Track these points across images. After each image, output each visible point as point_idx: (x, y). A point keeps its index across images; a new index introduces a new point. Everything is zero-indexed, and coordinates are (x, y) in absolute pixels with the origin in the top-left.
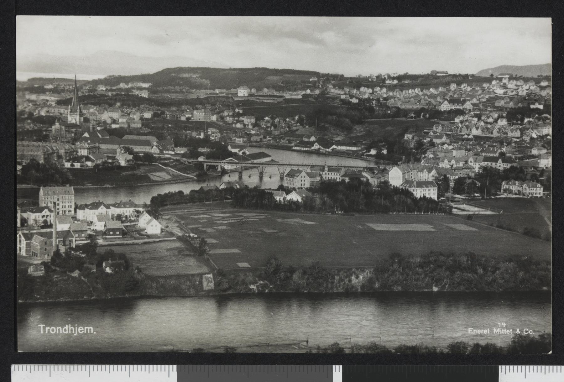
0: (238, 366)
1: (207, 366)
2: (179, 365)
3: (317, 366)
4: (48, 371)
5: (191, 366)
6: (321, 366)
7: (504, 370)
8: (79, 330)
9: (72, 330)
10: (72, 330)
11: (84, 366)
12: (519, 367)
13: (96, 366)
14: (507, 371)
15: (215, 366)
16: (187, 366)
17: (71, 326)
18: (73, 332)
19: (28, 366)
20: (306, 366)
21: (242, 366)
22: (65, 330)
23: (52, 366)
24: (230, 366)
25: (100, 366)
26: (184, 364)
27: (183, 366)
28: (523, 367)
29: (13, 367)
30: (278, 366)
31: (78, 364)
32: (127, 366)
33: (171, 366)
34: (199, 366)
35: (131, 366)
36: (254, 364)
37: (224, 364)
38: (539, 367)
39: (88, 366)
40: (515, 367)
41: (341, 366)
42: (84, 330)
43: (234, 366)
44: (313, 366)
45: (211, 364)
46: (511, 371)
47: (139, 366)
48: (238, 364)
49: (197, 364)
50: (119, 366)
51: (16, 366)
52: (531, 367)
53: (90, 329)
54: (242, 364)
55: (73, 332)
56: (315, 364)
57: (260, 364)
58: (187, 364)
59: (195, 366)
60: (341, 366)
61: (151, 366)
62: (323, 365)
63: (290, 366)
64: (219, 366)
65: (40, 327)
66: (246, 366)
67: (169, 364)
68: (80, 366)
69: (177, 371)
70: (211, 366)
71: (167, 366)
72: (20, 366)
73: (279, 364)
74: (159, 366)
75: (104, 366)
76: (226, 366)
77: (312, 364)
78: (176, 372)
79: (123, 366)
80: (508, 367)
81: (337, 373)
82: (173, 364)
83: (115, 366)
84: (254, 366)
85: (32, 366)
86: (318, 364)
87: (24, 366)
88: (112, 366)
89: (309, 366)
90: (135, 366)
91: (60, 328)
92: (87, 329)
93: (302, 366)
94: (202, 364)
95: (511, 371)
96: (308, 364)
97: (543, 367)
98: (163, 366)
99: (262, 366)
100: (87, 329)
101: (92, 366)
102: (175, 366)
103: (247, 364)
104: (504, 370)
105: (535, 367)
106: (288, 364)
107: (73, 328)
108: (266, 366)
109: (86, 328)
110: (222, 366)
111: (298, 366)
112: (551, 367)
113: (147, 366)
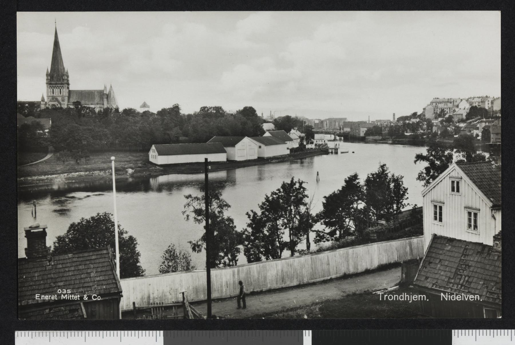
3: (289, 331)
4: (48, 337)
5: (176, 331)
6: (293, 331)
7: (456, 334)
8: (414, 297)
9: (407, 297)
10: (407, 297)
11: (80, 332)
12: (471, 331)
13: (91, 332)
14: (460, 334)
15: (197, 332)
16: (172, 331)
17: (406, 295)
18: (409, 299)
19: (30, 332)
20: (279, 331)
21: (222, 331)
22: (402, 298)
23: (51, 332)
24: (211, 332)
25: (94, 332)
26: (170, 329)
27: (169, 331)
29: (16, 333)
32: (119, 332)
33: (158, 332)
34: (183, 331)
35: (122, 332)
36: (233, 329)
37: (205, 330)
38: (488, 331)
39: (84, 332)
41: (311, 331)
42: (418, 298)
43: (215, 332)
45: (194, 330)
46: (463, 334)
47: (130, 332)
48: (218, 329)
49: (181, 330)
50: (112, 332)
51: (20, 332)
52: (481, 331)
53: (424, 297)
54: (222, 329)
55: (409, 299)
56: (287, 329)
57: (238, 329)
60: (311, 331)
61: (140, 332)
62: (295, 330)
63: (265, 331)
64: (201, 331)
66: (225, 331)
68: (76, 332)
69: (164, 336)
70: (194, 331)
71: (154, 332)
72: (23, 332)
73: (255, 330)
74: (147, 332)
75: (98, 332)
76: (208, 332)
78: (163, 337)
79: (115, 332)
80: (460, 331)
81: (307, 337)
82: (159, 329)
83: (108, 332)
84: (233, 331)
85: (34, 332)
87: (27, 332)
88: (105, 332)
90: (126, 332)
92: (421, 297)
93: (275, 331)
94: (186, 330)
95: (463, 334)
96: (282, 329)
97: (492, 331)
98: (151, 332)
99: (240, 331)
100: (421, 297)
101: (87, 332)
102: (162, 332)
103: (227, 329)
104: (456, 334)
106: (263, 330)
110: (204, 331)
111: (272, 331)
112: (499, 331)
113: (137, 332)
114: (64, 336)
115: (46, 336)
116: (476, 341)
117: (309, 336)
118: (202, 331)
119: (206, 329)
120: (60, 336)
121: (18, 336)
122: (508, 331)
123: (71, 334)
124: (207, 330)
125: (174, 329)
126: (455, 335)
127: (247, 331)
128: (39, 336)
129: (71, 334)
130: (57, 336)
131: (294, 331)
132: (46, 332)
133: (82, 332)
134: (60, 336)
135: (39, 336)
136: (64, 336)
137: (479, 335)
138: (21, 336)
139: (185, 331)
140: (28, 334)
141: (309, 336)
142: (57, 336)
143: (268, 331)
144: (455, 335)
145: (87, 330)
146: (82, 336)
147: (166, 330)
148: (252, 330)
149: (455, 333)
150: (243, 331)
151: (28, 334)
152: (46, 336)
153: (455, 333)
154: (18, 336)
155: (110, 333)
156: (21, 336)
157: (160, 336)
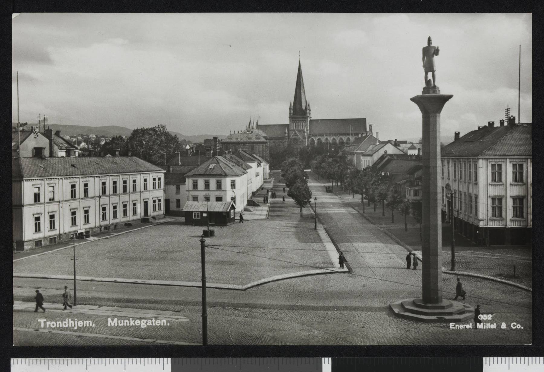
0: (231, 358)
1: (200, 359)
3: (307, 359)
4: (47, 364)
5: (185, 359)
6: (311, 359)
7: (488, 362)
11: (81, 359)
13: (92, 359)
14: (492, 362)
15: (208, 359)
16: (181, 359)
20: (296, 359)
21: (235, 359)
23: (46, 359)
24: (223, 359)
25: (96, 359)
26: (177, 357)
27: (177, 359)
28: (507, 358)
29: (13, 360)
30: (269, 359)
32: (123, 359)
33: (165, 359)
34: (192, 359)
35: (127, 359)
38: (522, 358)
39: (85, 359)
40: (499, 358)
43: (227, 359)
45: (204, 357)
47: (135, 359)
49: (190, 357)
50: (115, 359)
51: (15, 359)
52: (515, 358)
56: (305, 356)
57: (251, 357)
58: (181, 357)
59: (188, 359)
61: (146, 359)
64: (211, 359)
65: (40, 323)
66: (238, 359)
67: (163, 357)
68: (77, 359)
69: (171, 364)
70: (204, 359)
71: (162, 359)
72: (19, 359)
73: (270, 357)
74: (154, 359)
75: (100, 359)
76: (219, 359)
77: (302, 357)
78: (171, 365)
79: (119, 359)
81: (327, 365)
82: (167, 357)
85: (31, 359)
86: (308, 357)
87: (23, 359)
88: (108, 359)
90: (131, 359)
91: (60, 322)
93: (292, 359)
97: (526, 358)
98: (158, 359)
99: (254, 359)
102: (169, 359)
103: (240, 356)
104: (488, 362)
105: (519, 358)
106: (279, 357)
107: (73, 322)
109: (85, 322)
110: (215, 359)
112: (534, 358)
113: (142, 359)
114: (64, 364)
115: (44, 364)
116: (509, 369)
117: (329, 364)
119: (218, 356)
120: (60, 364)
123: (71, 362)
126: (486, 363)
127: (261, 359)
128: (37, 364)
129: (71, 362)
130: (56, 364)
132: (44, 360)
133: (83, 359)
135: (37, 364)
136: (64, 364)
137: (513, 363)
138: (18, 364)
139: (195, 358)
141: (329, 364)
142: (56, 364)
144: (486, 363)
145: (88, 357)
146: (83, 364)
147: (174, 357)
148: (267, 357)
149: (486, 360)
150: (257, 359)
152: (44, 364)
153: (486, 360)
155: (113, 360)
156: (18, 364)
157: (167, 364)
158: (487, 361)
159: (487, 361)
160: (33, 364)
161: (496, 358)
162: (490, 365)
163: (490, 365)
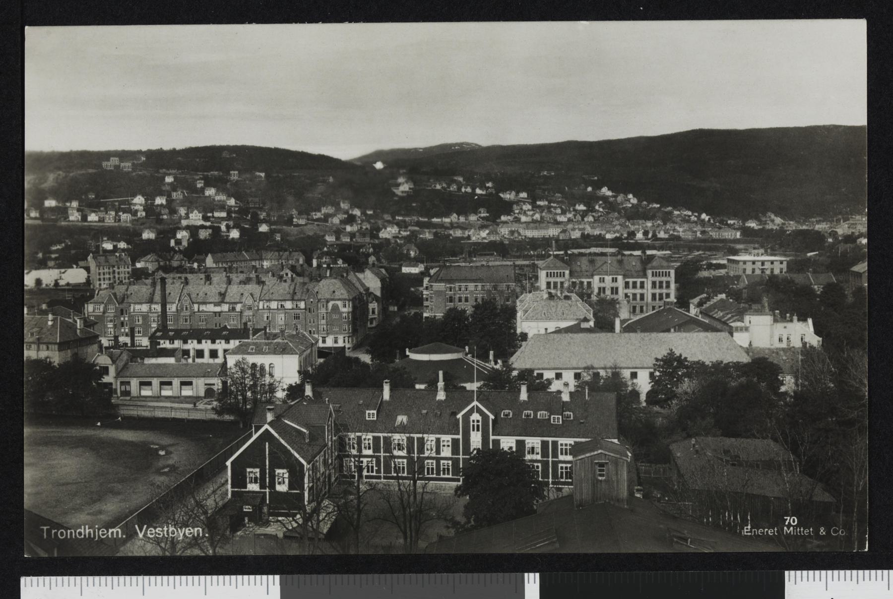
0: (376, 575)
1: (327, 577)
2: (284, 576)
3: (501, 575)
4: (78, 586)
5: (302, 577)
7: (792, 578)
12: (817, 572)
14: (799, 579)
15: (339, 576)
16: (296, 576)
19: (47, 578)
20: (482, 575)
21: (383, 576)
24: (364, 576)
27: (290, 577)
29: (23, 580)
31: (125, 575)
32: (202, 577)
33: (271, 577)
34: (314, 576)
35: (209, 577)
38: (848, 572)
39: (140, 578)
40: (811, 572)
41: (537, 575)
43: (370, 576)
44: (494, 575)
46: (805, 579)
48: (376, 572)
49: (311, 573)
51: (28, 579)
54: (382, 573)
58: (297, 574)
59: (308, 577)
60: (537, 575)
63: (457, 575)
64: (345, 576)
66: (389, 576)
67: (267, 574)
68: (128, 578)
69: (280, 585)
70: (333, 576)
72: (35, 579)
73: (439, 573)
76: (358, 576)
78: (279, 587)
81: (532, 584)
82: (274, 573)
84: (401, 576)
88: (178, 577)
89: (488, 575)
90: (215, 577)
93: (476, 575)
94: (319, 573)
95: (805, 579)
98: (258, 577)
99: (413, 576)
101: (147, 578)
102: (277, 577)
103: (391, 572)
104: (792, 578)
106: (453, 573)
108: (419, 576)
112: (867, 572)
117: (535, 583)
118: (347, 575)
120: (100, 586)
121: (25, 586)
122: (882, 572)
124: (357, 573)
125: (299, 573)
126: (789, 581)
127: (426, 575)
128: (63, 586)
129: (119, 582)
131: (502, 574)
134: (100, 586)
135: (63, 586)
136: (106, 585)
137: (833, 580)
138: (32, 586)
140: (44, 581)
141: (535, 583)
143: (463, 575)
144: (789, 581)
149: (789, 576)
151: (44, 581)
152: (75, 586)
153: (789, 576)
154: (25, 586)
156: (32, 586)
157: (274, 584)
158: (790, 576)
159: (790, 576)
160: (56, 586)
161: (805, 572)
162: (796, 584)
163: (796, 584)
